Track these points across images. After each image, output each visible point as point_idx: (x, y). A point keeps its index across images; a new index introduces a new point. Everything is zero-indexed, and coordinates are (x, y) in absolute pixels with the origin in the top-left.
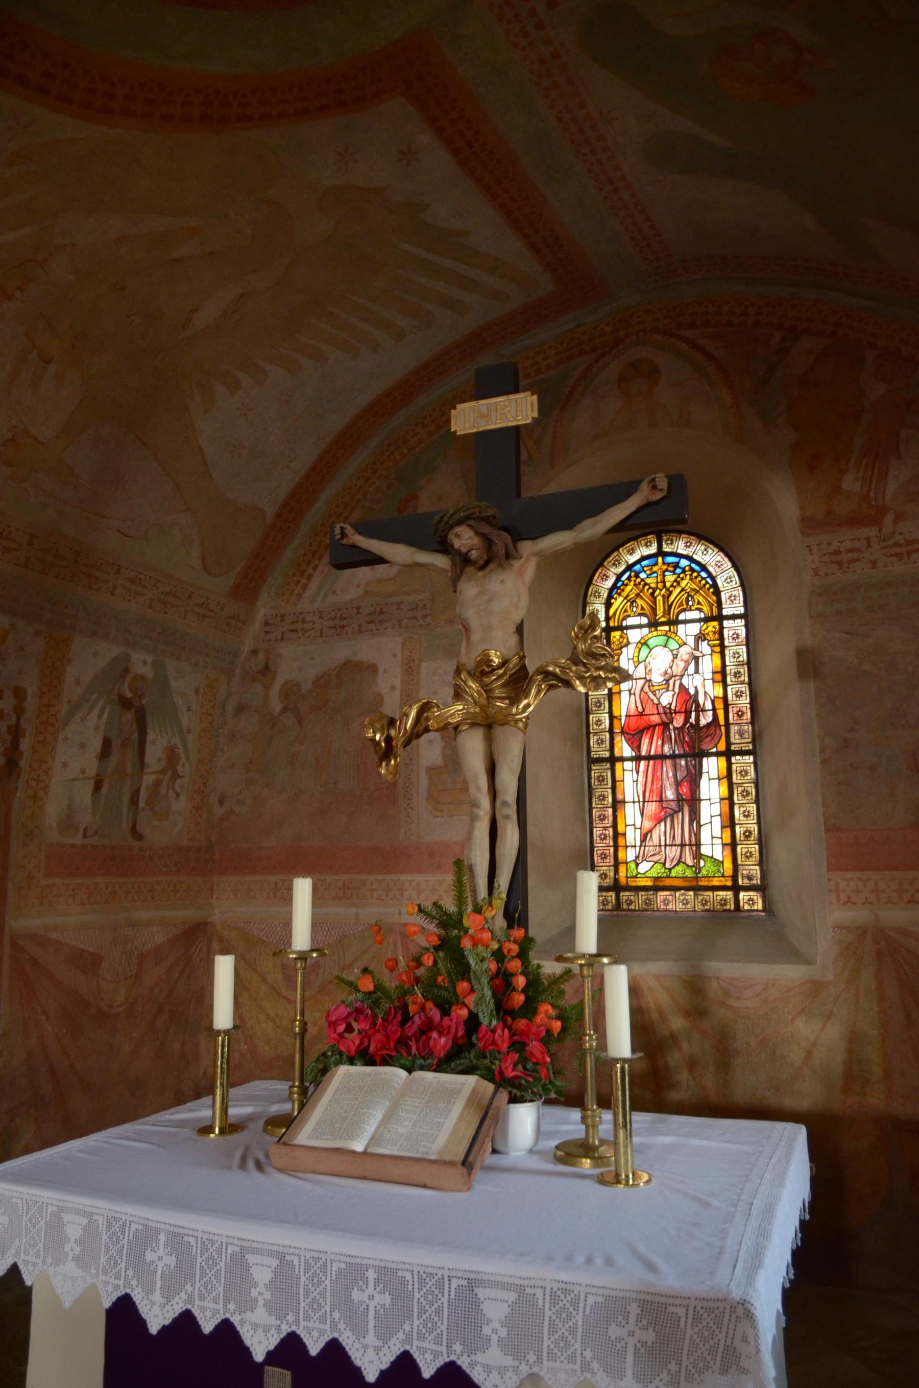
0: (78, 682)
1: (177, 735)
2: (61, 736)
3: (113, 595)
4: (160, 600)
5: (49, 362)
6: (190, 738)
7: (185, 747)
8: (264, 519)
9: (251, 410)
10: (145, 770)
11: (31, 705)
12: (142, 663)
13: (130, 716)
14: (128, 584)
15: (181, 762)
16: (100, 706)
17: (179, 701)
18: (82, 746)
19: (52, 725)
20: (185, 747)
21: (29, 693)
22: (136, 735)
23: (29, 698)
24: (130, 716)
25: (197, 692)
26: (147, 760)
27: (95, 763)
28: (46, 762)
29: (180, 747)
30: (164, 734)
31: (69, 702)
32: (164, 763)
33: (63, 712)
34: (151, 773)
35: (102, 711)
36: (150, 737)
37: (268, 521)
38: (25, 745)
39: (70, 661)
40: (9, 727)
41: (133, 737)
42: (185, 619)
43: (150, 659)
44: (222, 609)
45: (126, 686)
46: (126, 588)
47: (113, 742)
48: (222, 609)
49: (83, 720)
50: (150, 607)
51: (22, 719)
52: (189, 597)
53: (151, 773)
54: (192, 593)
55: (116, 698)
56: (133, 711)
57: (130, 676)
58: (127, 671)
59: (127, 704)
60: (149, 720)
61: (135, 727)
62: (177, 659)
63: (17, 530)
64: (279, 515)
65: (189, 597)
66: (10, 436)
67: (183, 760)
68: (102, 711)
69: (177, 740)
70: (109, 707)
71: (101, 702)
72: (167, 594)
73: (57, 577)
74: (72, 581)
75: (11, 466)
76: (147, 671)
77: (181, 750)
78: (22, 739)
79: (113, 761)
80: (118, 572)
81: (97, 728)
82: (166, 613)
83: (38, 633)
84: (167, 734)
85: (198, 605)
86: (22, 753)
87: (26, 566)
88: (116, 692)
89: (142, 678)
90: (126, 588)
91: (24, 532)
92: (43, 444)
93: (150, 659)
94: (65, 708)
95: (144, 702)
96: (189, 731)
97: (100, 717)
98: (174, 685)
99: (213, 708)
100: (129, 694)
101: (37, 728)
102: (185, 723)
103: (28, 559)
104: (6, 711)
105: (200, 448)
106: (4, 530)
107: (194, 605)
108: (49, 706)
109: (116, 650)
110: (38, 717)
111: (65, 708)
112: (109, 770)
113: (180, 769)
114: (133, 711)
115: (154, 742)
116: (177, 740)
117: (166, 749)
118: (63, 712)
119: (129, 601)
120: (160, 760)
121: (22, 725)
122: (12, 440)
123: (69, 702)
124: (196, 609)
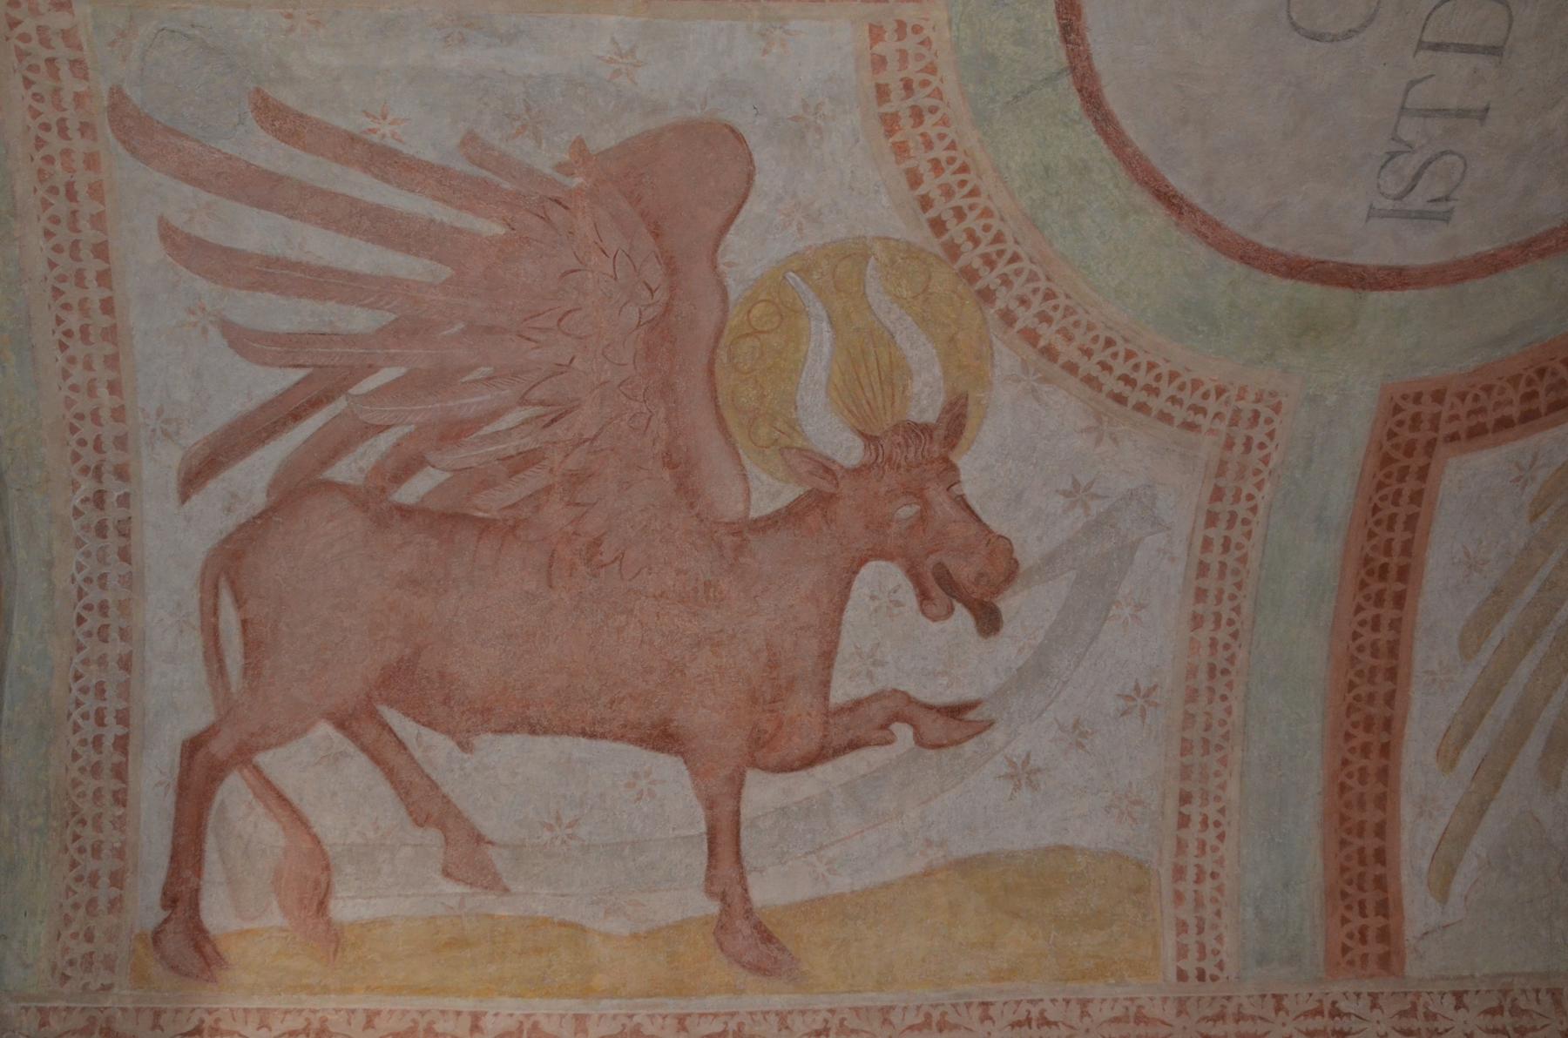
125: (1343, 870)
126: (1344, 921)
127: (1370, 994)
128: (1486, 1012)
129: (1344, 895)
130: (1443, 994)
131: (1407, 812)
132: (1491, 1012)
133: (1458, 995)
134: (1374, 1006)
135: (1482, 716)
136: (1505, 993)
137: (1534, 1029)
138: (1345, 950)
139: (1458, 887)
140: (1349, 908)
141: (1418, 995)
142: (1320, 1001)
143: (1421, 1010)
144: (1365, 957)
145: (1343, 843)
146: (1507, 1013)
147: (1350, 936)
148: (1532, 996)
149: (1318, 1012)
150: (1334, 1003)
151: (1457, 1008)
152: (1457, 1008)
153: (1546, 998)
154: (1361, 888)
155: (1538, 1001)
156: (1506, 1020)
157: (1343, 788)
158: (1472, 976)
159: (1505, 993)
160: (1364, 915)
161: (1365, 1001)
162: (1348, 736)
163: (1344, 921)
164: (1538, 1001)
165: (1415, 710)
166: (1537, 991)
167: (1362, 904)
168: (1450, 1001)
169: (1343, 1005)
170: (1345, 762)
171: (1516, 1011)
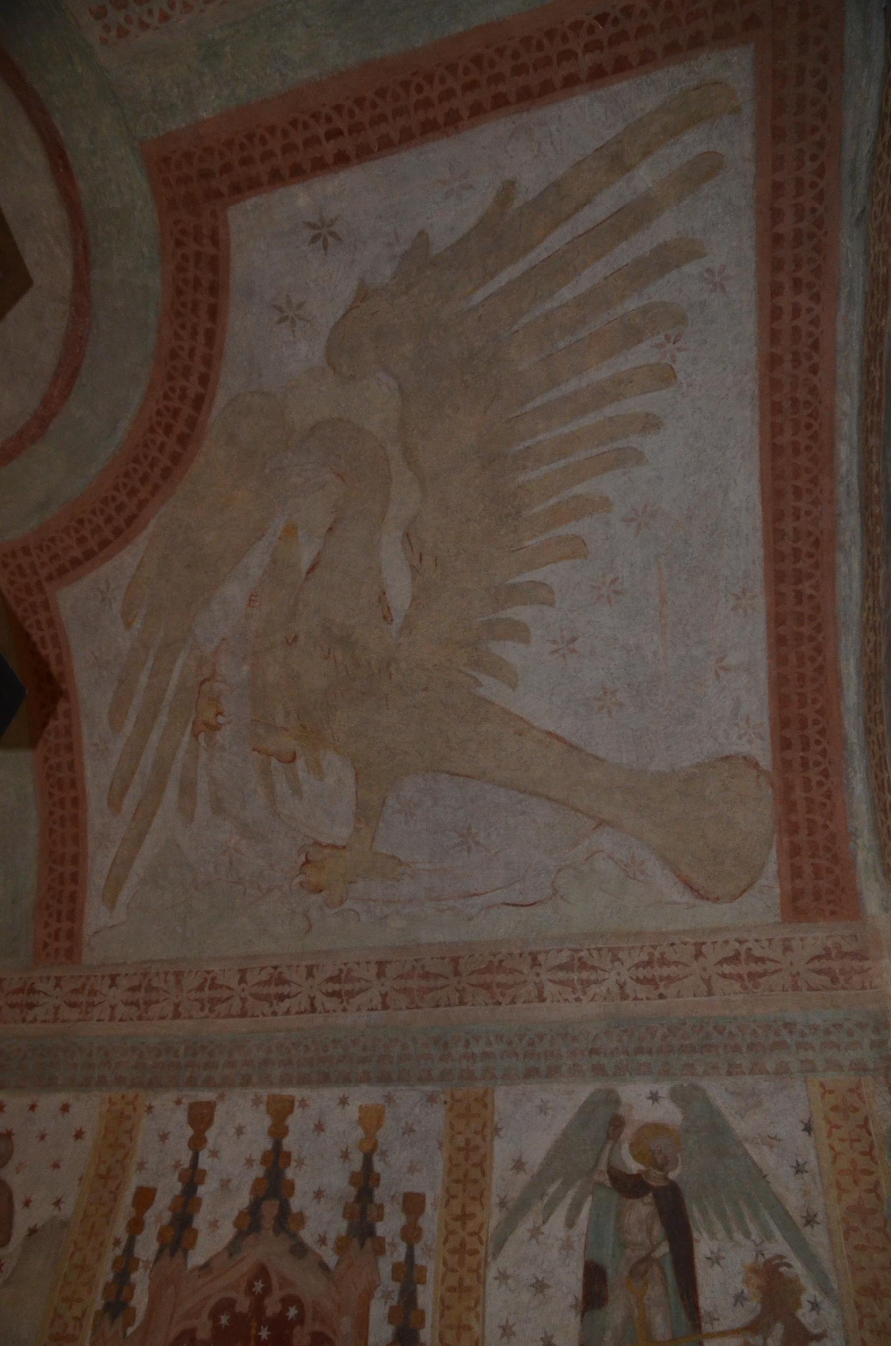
0: (519, 1165)
1: (778, 1234)
2: (492, 1273)
3: (544, 1000)
4: (638, 980)
5: (293, 759)
6: (817, 1237)
7: (811, 1261)
8: (756, 765)
9: (574, 640)
10: (706, 1328)
11: (431, 1222)
12: (645, 1102)
13: (642, 1210)
14: (561, 975)
15: (805, 1298)
16: (568, 1201)
17: (766, 1158)
18: (540, 1286)
19: (475, 1252)
20: (811, 1261)
21: (428, 1202)
22: (664, 1249)
23: (428, 1209)
24: (642, 1210)
25: (808, 1128)
26: (705, 1303)
27: (573, 1321)
28: (470, 1328)
29: (792, 1258)
30: (738, 1236)
31: (503, 1204)
32: (754, 1305)
33: (493, 1223)
34: (723, 1334)
35: (576, 1208)
36: (703, 1247)
37: (766, 763)
38: (426, 1297)
39: (496, 1130)
40: (396, 1268)
41: (657, 1254)
42: (710, 993)
43: (664, 1088)
44: (787, 949)
45: (625, 1149)
46: (562, 983)
47: (610, 1272)
48: (787, 949)
49: (535, 1233)
50: (624, 997)
51: (418, 1252)
52: (699, 954)
53: (723, 1334)
54: (699, 945)
55: (606, 1179)
56: (649, 1198)
57: (628, 1133)
58: (617, 1123)
59: (629, 1186)
60: (694, 1211)
61: (658, 1230)
62: (729, 1073)
63: (358, 964)
64: (783, 744)
65: (699, 954)
66: (303, 858)
67: (810, 1292)
68: (576, 1208)
69: (779, 1246)
70: (590, 1198)
71: (572, 1193)
72: (648, 964)
73: (437, 1006)
74: (462, 1003)
75: (320, 891)
76: (668, 1113)
77: (798, 1268)
78: (420, 1287)
79: (615, 1313)
80: (535, 961)
81: (567, 1246)
82: (661, 996)
83: (431, 1099)
84: (747, 1234)
85: (725, 960)
86: (423, 1312)
87: (385, 1007)
88: (603, 1167)
89: (658, 1128)
90: (562, 983)
91: (368, 963)
92: (344, 847)
93: (664, 1088)
94: (495, 1218)
95: (672, 1175)
96: (810, 1220)
97: (570, 1223)
98: (741, 1127)
99: (869, 1153)
100: (634, 1167)
101: (445, 1263)
102: (793, 1203)
103: (384, 996)
104: (388, 1240)
105: (550, 734)
106: (341, 971)
107: (720, 963)
108: (464, 1217)
109: (584, 1092)
110: (445, 1241)
111: (495, 1218)
112: (609, 1333)
113: (806, 1316)
114: (649, 1198)
115: (715, 1260)
116: (779, 1246)
117: (755, 1270)
118: (493, 1223)
119: (578, 1000)
120: (739, 1298)
121: (420, 1261)
122: (308, 861)
123: (503, 1204)
124: (727, 969)
125: (50, 888)
126: (47, 925)
127: (56, 978)
128: (129, 990)
129: (48, 907)
130: (103, 977)
131: (91, 846)
132: (134, 989)
133: (113, 978)
134: (57, 985)
135: (133, 773)
136: (144, 975)
137: (157, 1002)
138: (45, 945)
139: (124, 897)
140: (50, 915)
141: (88, 977)
142: (25, 983)
143: (88, 988)
144: (57, 950)
145: (51, 870)
146: (143, 990)
147: (49, 936)
148: (162, 976)
149: (20, 991)
150: (33, 983)
151: (111, 987)
152: (111, 987)
153: (171, 978)
154: (59, 902)
155: (166, 981)
156: (141, 996)
157: (51, 831)
158: (125, 963)
159: (144, 975)
160: (59, 920)
161: (52, 983)
162: (51, 795)
163: (47, 925)
164: (166, 981)
165: (88, 773)
166: (166, 973)
167: (59, 913)
168: (108, 981)
169: (38, 986)
170: (51, 813)
171: (150, 989)
